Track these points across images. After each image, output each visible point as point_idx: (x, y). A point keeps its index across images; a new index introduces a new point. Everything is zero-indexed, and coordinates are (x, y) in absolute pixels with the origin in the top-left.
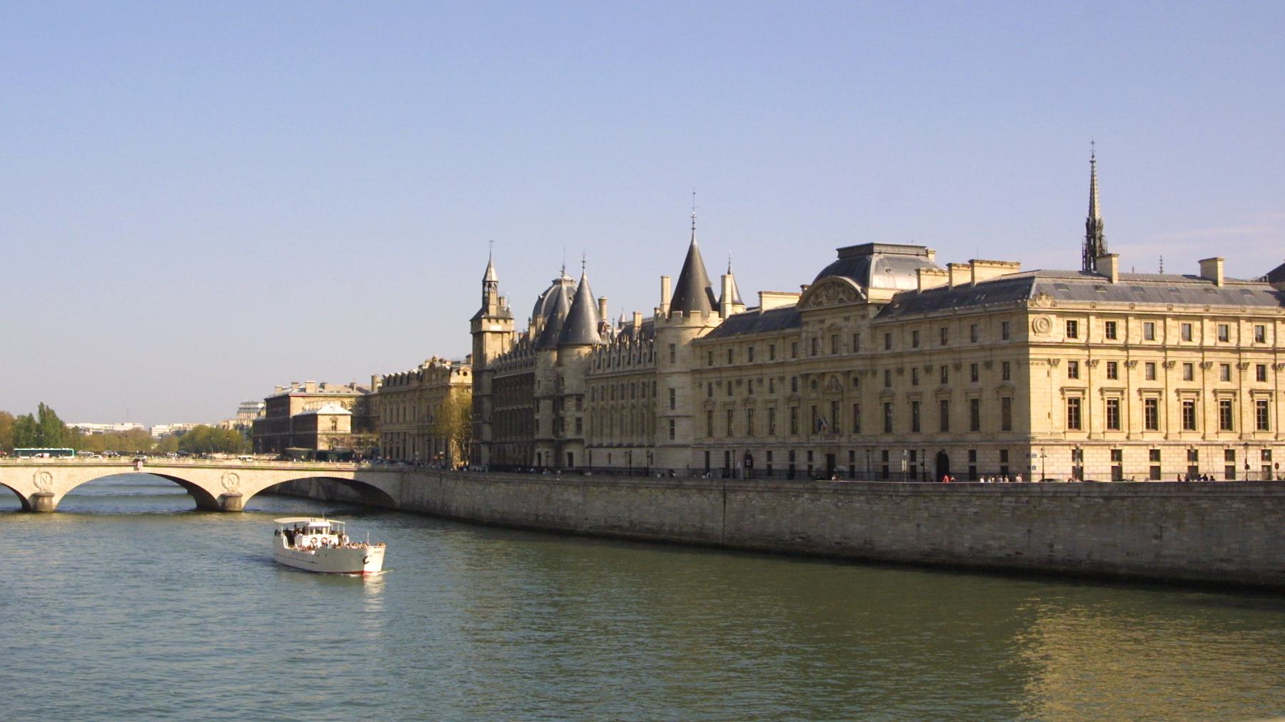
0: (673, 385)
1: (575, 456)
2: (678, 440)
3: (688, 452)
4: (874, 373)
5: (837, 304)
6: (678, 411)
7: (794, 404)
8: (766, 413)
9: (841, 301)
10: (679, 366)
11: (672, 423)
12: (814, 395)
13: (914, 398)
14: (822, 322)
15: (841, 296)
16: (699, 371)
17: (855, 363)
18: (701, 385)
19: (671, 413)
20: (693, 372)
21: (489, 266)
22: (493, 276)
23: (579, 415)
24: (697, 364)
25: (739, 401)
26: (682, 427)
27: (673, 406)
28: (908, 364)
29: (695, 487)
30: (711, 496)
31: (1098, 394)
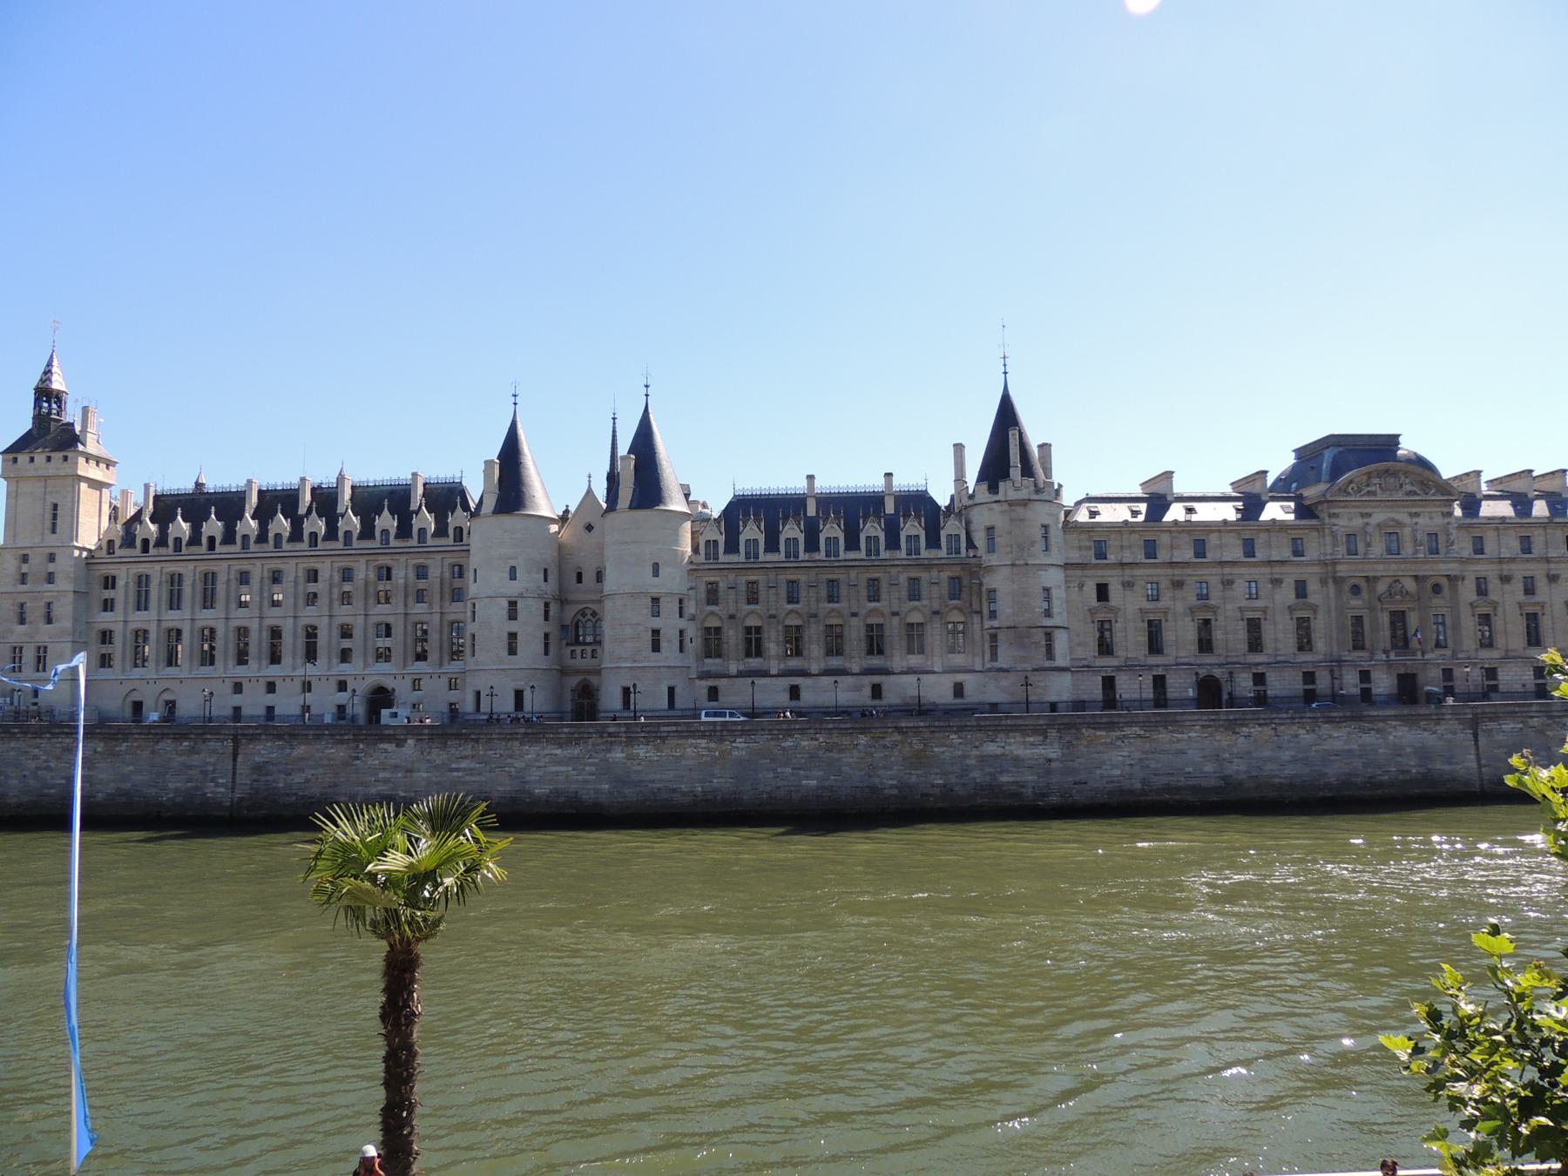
0: (1048, 585)
1: (678, 690)
2: (1060, 661)
3: (1067, 677)
5: (1399, 496)
6: (1056, 620)
7: (1304, 614)
8: (1242, 626)
9: (1409, 493)
10: (1056, 557)
11: (1049, 637)
12: (1355, 602)
13: (1531, 610)
14: (1369, 515)
15: (1408, 488)
16: (1082, 566)
18: (1081, 586)
19: (1047, 622)
20: (1067, 566)
21: (50, 364)
22: (57, 384)
23: (682, 624)
24: (1075, 557)
25: (1180, 607)
26: (1061, 641)
27: (1048, 613)
28: (1519, 571)
29: (1396, 718)
30: (1441, 729)
31: (1469, 609)
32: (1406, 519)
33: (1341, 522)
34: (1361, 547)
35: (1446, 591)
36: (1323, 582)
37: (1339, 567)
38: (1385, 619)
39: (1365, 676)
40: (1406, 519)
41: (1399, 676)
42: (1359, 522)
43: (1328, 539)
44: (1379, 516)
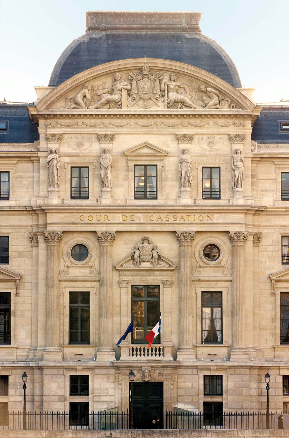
4: (258, 238)
15: (173, 96)
17: (217, 219)
32: (170, 145)
33: (64, 149)
34: (94, 188)
35: (225, 257)
36: (34, 239)
37: (52, 218)
38: (124, 298)
39: (79, 384)
40: (170, 145)
41: (134, 386)
42: (94, 148)
43: (43, 175)
44: (127, 140)
